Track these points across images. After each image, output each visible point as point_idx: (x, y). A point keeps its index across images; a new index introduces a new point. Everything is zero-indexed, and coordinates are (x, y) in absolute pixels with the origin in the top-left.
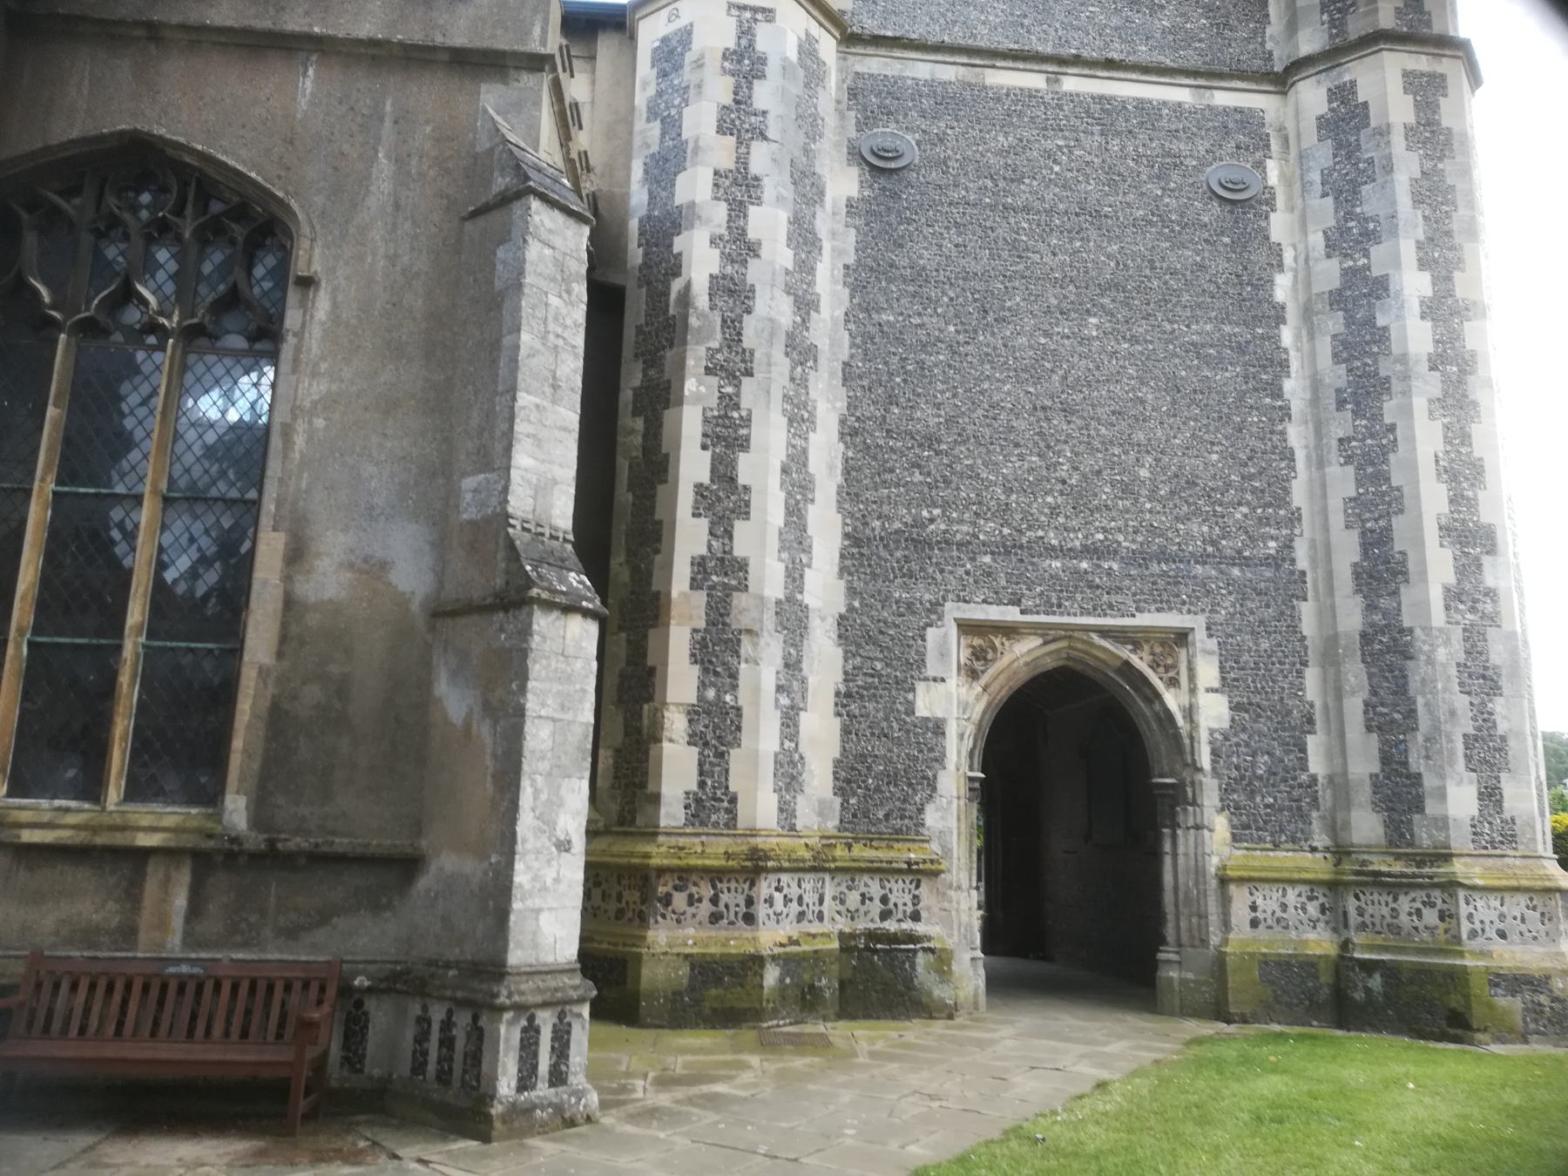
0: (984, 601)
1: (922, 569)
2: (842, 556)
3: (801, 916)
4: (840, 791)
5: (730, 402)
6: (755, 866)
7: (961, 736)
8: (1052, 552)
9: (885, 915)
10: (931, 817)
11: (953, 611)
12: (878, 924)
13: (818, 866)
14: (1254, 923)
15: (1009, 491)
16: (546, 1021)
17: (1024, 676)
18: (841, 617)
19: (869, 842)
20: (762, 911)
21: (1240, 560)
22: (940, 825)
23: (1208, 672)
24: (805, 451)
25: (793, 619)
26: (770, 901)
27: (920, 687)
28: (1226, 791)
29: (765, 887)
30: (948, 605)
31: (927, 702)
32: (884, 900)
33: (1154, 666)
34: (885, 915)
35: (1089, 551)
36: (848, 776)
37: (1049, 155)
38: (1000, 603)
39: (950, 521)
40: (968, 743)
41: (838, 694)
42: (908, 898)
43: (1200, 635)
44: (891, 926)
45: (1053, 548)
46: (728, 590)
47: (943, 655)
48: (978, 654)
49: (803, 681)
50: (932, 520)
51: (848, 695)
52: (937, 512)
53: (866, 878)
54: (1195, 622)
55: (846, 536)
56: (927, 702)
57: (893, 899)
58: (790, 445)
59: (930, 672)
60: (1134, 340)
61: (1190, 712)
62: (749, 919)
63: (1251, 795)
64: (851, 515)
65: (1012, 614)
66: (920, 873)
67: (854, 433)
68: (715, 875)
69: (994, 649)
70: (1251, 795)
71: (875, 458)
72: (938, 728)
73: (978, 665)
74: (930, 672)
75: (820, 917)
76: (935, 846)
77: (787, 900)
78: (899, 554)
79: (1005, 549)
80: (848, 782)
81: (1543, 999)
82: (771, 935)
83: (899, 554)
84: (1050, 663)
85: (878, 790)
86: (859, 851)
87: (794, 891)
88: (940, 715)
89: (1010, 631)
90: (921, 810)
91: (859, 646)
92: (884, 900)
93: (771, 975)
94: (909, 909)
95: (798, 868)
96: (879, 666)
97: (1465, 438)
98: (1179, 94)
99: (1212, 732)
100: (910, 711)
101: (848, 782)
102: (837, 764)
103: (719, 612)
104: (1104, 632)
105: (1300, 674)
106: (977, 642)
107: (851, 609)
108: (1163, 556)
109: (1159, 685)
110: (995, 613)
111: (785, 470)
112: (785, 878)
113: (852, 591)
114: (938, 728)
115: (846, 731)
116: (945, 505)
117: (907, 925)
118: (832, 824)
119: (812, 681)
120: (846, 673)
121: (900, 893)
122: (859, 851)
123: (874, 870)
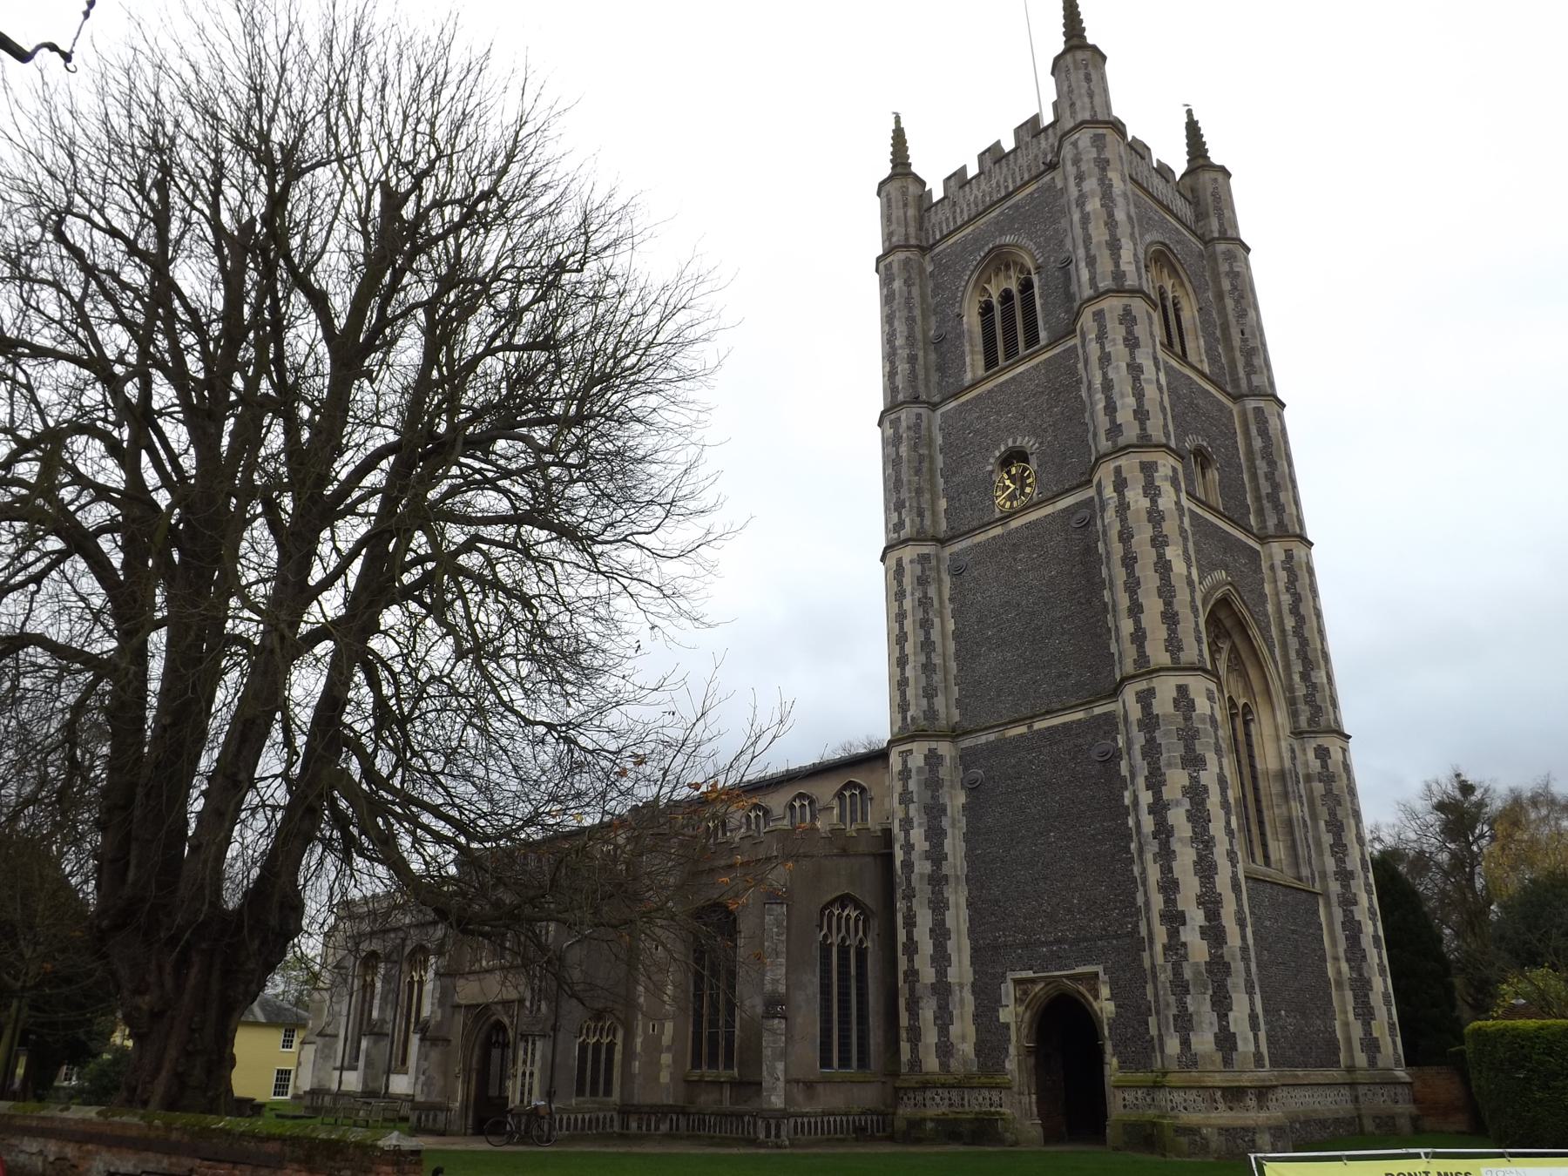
4: (976, 1055)
5: (910, 909)
6: (925, 1086)
7: (1018, 1030)
8: (1044, 944)
9: (991, 1105)
10: (1008, 1065)
11: (1010, 975)
14: (1125, 1106)
15: (1025, 919)
20: (928, 1103)
21: (1117, 937)
23: (1105, 991)
28: (1115, 1046)
29: (929, 1094)
33: (1089, 991)
34: (991, 1105)
35: (1058, 941)
37: (1031, 762)
39: (1005, 936)
40: (1024, 1032)
43: (1101, 974)
44: (993, 1109)
47: (1007, 995)
48: (1025, 993)
54: (1099, 969)
60: (1068, 839)
61: (1101, 1009)
63: (1126, 1047)
65: (1030, 974)
68: (914, 1089)
70: (1126, 1047)
72: (1007, 1026)
75: (963, 1105)
79: (1026, 945)
81: (1198, 1138)
82: (931, 1112)
89: (1033, 981)
93: (930, 1125)
97: (1170, 870)
98: (1080, 715)
99: (1108, 1019)
103: (912, 991)
104: (1067, 977)
105: (1144, 987)
108: (1085, 939)
109: (1091, 999)
112: (940, 1091)
113: (975, 972)
114: (1007, 1026)
116: (1004, 930)
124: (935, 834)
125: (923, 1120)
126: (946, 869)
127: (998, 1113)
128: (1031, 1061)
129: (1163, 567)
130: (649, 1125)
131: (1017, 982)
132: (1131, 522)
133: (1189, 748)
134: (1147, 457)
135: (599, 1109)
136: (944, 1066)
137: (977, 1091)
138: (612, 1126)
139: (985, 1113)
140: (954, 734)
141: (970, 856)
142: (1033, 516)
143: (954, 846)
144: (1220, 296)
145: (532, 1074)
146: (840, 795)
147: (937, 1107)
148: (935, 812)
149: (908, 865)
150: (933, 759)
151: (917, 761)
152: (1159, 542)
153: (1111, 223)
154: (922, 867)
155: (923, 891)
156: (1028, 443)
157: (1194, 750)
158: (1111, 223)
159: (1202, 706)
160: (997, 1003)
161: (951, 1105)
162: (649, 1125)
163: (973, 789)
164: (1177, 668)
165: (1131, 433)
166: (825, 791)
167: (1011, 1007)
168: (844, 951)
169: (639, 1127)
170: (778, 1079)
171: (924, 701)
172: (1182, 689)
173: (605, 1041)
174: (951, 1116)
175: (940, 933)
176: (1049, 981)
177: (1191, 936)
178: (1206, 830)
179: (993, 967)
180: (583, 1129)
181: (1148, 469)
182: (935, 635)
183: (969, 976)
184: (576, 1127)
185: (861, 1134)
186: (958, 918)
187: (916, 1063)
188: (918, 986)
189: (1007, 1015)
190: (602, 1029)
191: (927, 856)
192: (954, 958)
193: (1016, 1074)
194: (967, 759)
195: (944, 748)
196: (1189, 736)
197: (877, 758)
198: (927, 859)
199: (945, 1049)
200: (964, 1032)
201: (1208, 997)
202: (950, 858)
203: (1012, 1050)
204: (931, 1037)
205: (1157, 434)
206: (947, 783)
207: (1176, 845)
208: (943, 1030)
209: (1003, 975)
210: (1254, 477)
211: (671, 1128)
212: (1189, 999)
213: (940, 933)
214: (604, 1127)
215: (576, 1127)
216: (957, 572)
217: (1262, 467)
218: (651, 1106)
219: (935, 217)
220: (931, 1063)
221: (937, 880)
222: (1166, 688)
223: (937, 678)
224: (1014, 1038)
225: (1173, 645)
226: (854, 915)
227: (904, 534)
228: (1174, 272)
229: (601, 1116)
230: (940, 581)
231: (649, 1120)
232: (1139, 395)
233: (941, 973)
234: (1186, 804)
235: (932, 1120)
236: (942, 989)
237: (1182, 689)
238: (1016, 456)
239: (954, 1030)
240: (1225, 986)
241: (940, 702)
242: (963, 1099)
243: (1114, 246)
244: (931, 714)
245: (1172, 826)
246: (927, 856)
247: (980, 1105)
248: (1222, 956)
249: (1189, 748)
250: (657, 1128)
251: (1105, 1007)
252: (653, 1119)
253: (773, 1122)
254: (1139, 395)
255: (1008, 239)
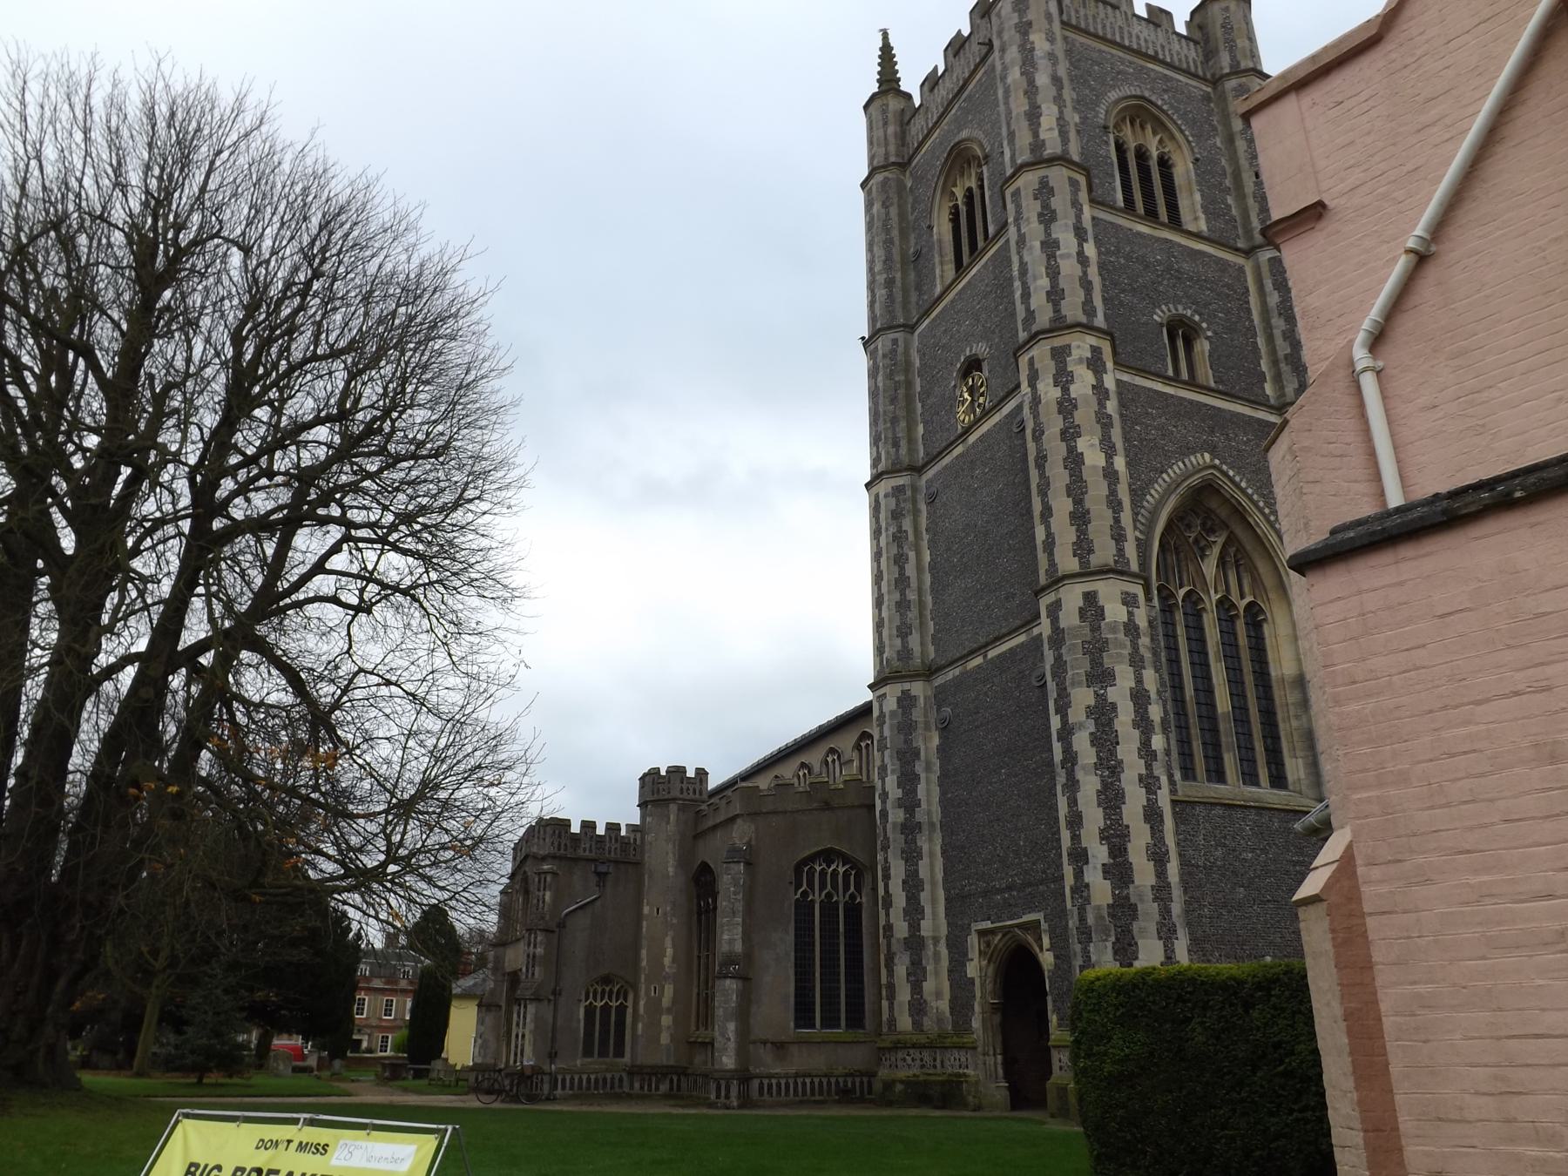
4: (951, 1014)
6: (898, 1046)
7: (983, 985)
14: (1061, 1068)
20: (900, 1063)
23: (1046, 941)
29: (900, 1055)
35: (1010, 888)
37: (986, 694)
40: (989, 987)
48: (988, 945)
60: (1016, 776)
68: (890, 1049)
72: (973, 979)
75: (935, 1067)
82: (902, 1074)
89: (992, 932)
93: (899, 1087)
98: (1022, 638)
108: (1030, 884)
112: (911, 1051)
124: (908, 780)
125: (894, 1082)
126: (920, 815)
128: (997, 1019)
129: (1074, 461)
130: (650, 1086)
132: (1043, 418)
133: (1096, 662)
134: (1058, 342)
135: (607, 1070)
136: (917, 1025)
138: (621, 1086)
140: (929, 672)
141: (944, 802)
142: (985, 427)
143: (928, 792)
144: (1230, 140)
145: (523, 1036)
146: (858, 747)
147: (906, 1069)
148: (908, 756)
149: (884, 814)
150: (906, 701)
151: (891, 704)
152: (1070, 434)
153: (1031, 90)
154: (896, 816)
155: (896, 840)
156: (981, 349)
157: (1102, 664)
158: (1031, 90)
159: (1115, 612)
161: (922, 1066)
162: (650, 1086)
163: (945, 728)
164: (1086, 573)
165: (1044, 318)
166: (846, 742)
167: (976, 960)
168: (829, 908)
169: (642, 1088)
170: (729, 1039)
171: (898, 642)
172: (1090, 597)
173: (614, 1004)
174: (921, 1078)
175: (913, 885)
176: (1006, 931)
177: (1094, 877)
178: (1112, 753)
180: (588, 1088)
181: (1060, 355)
182: (910, 570)
183: (944, 930)
184: (580, 1087)
185: (846, 1096)
186: (932, 868)
187: (892, 1021)
189: (972, 970)
190: (611, 992)
191: (900, 803)
192: (928, 910)
193: (981, 1032)
194: (940, 697)
195: (917, 688)
196: (1096, 649)
197: (864, 712)
198: (900, 807)
199: (918, 1007)
200: (937, 985)
201: (1109, 945)
202: (924, 805)
203: (977, 1008)
204: (904, 995)
205: (1072, 309)
206: (921, 725)
207: (1080, 775)
208: (917, 987)
210: (1270, 339)
211: (671, 1089)
212: (1092, 948)
213: (913, 885)
214: (612, 1087)
215: (580, 1087)
216: (932, 499)
217: (1279, 324)
218: (652, 1067)
219: (917, 127)
220: (905, 1022)
221: (910, 829)
222: (1072, 597)
223: (912, 615)
224: (978, 994)
225: (1083, 547)
226: (841, 870)
227: (881, 467)
228: (1159, 126)
229: (609, 1076)
230: (916, 513)
231: (650, 1080)
232: (1053, 273)
233: (914, 927)
234: (1091, 726)
235: (902, 1082)
236: (915, 943)
237: (1090, 597)
238: (973, 365)
239: (928, 986)
240: (1130, 931)
241: (914, 641)
242: (935, 1060)
243: (1034, 116)
244: (905, 654)
245: (1076, 753)
246: (900, 803)
248: (1127, 898)
249: (1096, 662)
250: (657, 1088)
251: (1047, 959)
252: (654, 1079)
253: (723, 1083)
254: (1053, 273)
255: (964, 134)
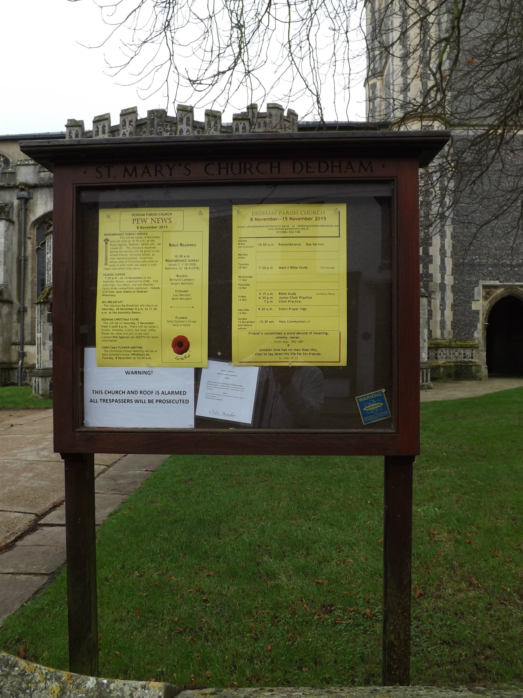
0: (490, 280)
1: (473, 272)
2: (452, 270)
3: (446, 358)
4: (452, 329)
7: (483, 314)
9: (465, 358)
11: (482, 283)
12: (463, 359)
13: (449, 347)
15: (496, 250)
16: (425, 370)
17: (499, 298)
18: (453, 285)
19: (460, 341)
20: (439, 356)
22: (478, 336)
24: (444, 244)
25: (442, 287)
26: (440, 354)
27: (473, 303)
29: (439, 351)
30: (480, 281)
31: (475, 306)
32: (464, 354)
34: (465, 358)
36: (455, 325)
38: (494, 280)
39: (481, 259)
40: (485, 316)
41: (452, 305)
42: (470, 354)
44: (466, 360)
45: (508, 265)
46: (428, 282)
47: (479, 294)
48: (488, 293)
49: (445, 303)
50: (476, 259)
51: (455, 305)
52: (477, 257)
53: (460, 349)
55: (453, 264)
56: (475, 306)
57: (466, 354)
58: (441, 243)
59: (476, 299)
62: (436, 358)
64: (454, 259)
65: (497, 283)
66: (472, 347)
67: (455, 237)
69: (492, 291)
71: (460, 243)
72: (477, 312)
73: (488, 296)
74: (476, 299)
75: (450, 358)
76: (476, 341)
77: (444, 354)
78: (467, 268)
79: (495, 266)
80: (455, 326)
83: (467, 268)
84: (506, 295)
85: (462, 328)
86: (458, 343)
87: (445, 352)
88: (478, 309)
89: (496, 287)
90: (473, 333)
91: (457, 293)
92: (464, 354)
93: (442, 370)
94: (470, 356)
95: (446, 347)
96: (462, 297)
100: (470, 308)
101: (455, 326)
102: (452, 322)
106: (487, 290)
107: (455, 283)
110: (492, 283)
111: (440, 250)
112: (443, 349)
113: (455, 279)
115: (454, 314)
116: (479, 255)
117: (470, 360)
118: (451, 337)
119: (447, 302)
120: (454, 300)
121: (468, 352)
122: (458, 343)
123: (461, 347)
125: (439, 367)
127: (471, 362)
131: (485, 287)
137: (455, 350)
139: (461, 362)
160: (471, 298)
174: (448, 364)
179: (469, 277)
188: (431, 284)
209: (477, 283)
247: (457, 358)
